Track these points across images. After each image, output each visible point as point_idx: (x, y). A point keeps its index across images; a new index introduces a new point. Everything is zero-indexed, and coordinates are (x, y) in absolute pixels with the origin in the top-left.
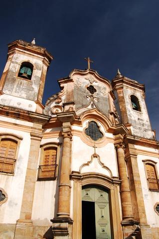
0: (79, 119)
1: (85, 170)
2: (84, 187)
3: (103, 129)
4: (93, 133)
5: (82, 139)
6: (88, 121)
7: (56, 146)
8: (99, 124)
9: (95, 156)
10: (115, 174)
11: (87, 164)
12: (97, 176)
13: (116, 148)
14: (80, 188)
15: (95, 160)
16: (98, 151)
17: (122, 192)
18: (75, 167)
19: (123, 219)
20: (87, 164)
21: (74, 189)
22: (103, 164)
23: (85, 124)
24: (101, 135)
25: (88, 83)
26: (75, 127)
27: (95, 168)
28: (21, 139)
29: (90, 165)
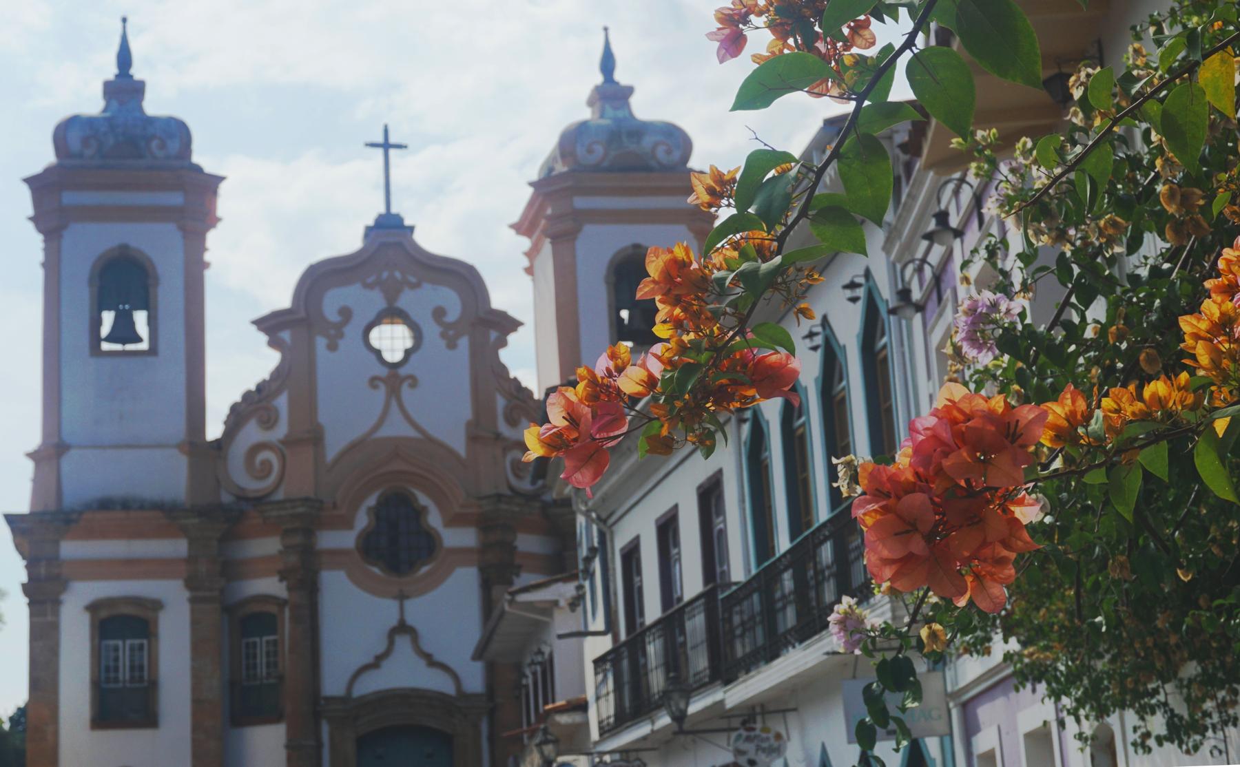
0: (335, 506)
3: (434, 519)
6: (372, 501)
7: (273, 609)
8: (423, 499)
9: (403, 628)
10: (474, 679)
13: (486, 586)
15: (403, 643)
17: (491, 739)
18: (333, 684)
23: (362, 521)
24: (428, 545)
26: (330, 540)
27: (405, 672)
28: (157, 605)
29: (385, 664)
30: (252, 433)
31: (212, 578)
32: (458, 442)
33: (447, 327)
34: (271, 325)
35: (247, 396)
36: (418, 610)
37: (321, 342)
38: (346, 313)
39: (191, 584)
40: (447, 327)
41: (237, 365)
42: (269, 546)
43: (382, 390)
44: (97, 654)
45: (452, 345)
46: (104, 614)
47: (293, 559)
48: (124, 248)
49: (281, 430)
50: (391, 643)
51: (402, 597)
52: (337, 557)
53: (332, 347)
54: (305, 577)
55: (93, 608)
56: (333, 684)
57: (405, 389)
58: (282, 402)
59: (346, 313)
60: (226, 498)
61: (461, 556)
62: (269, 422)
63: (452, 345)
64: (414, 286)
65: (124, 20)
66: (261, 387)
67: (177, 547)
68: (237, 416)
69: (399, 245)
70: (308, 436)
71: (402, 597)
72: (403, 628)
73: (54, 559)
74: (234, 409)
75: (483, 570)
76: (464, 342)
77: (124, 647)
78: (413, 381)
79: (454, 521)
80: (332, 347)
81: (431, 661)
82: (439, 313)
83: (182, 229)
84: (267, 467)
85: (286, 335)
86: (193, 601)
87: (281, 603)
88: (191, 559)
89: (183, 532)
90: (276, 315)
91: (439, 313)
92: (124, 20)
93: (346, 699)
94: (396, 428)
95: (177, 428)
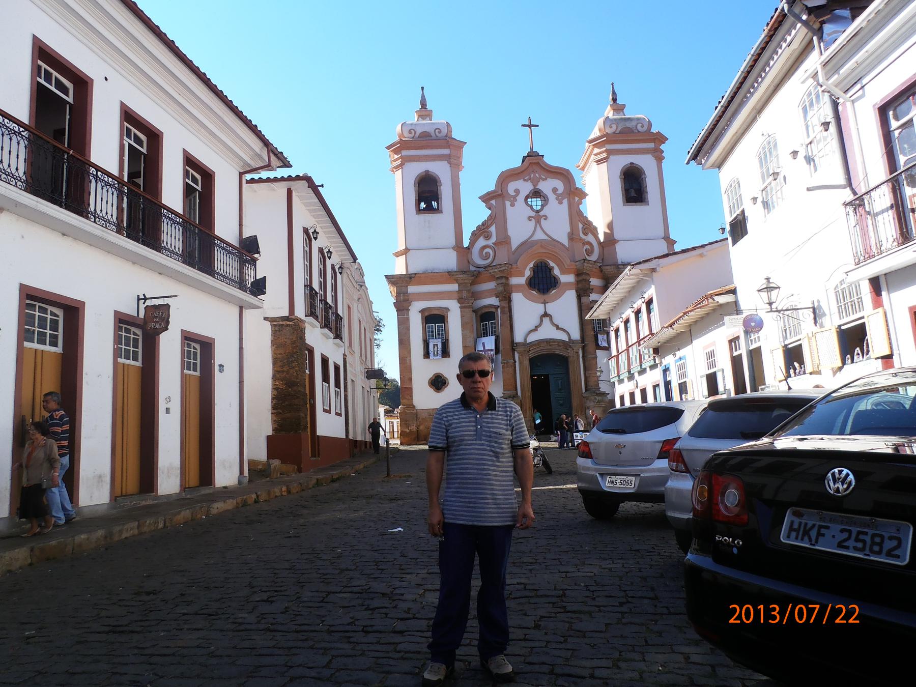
1: (532, 338)
2: (532, 361)
3: (556, 272)
4: (543, 282)
5: (525, 296)
6: (531, 265)
7: (493, 310)
8: (552, 264)
9: (546, 315)
10: (576, 335)
11: (536, 329)
12: (548, 342)
13: (579, 297)
14: (527, 363)
15: (546, 320)
16: (551, 308)
19: (586, 390)
20: (536, 329)
21: (520, 363)
22: (558, 327)
23: (528, 273)
25: (525, 187)
27: (547, 332)
28: (447, 309)
30: (481, 242)
31: (466, 298)
32: (565, 241)
33: (558, 195)
34: (487, 199)
35: (478, 227)
36: (551, 308)
37: (508, 203)
38: (517, 192)
39: (460, 300)
40: (558, 195)
41: (475, 214)
42: (491, 285)
43: (533, 222)
44: (424, 330)
45: (561, 203)
46: (426, 314)
47: (501, 288)
48: (427, 172)
49: (494, 239)
50: (542, 321)
51: (545, 303)
52: (518, 288)
53: (512, 205)
54: (506, 297)
55: (422, 311)
56: (519, 338)
57: (543, 221)
58: (493, 229)
59: (517, 192)
60: (472, 269)
61: (568, 286)
62: (488, 237)
63: (561, 203)
64: (543, 180)
65: (423, 88)
66: (483, 224)
67: (454, 287)
68: (475, 236)
69: (538, 163)
70: (504, 240)
71: (545, 303)
72: (546, 315)
73: (406, 293)
74: (474, 234)
75: (577, 291)
76: (565, 201)
77: (435, 327)
78: (546, 217)
79: (563, 272)
80: (512, 205)
81: (558, 327)
82: (555, 190)
83: (449, 163)
84: (487, 257)
85: (493, 202)
86: (461, 307)
87: (497, 307)
88: (460, 291)
89: (456, 281)
90: (488, 194)
91: (555, 190)
92: (423, 88)
93: (524, 344)
94: (540, 236)
95: (452, 241)
